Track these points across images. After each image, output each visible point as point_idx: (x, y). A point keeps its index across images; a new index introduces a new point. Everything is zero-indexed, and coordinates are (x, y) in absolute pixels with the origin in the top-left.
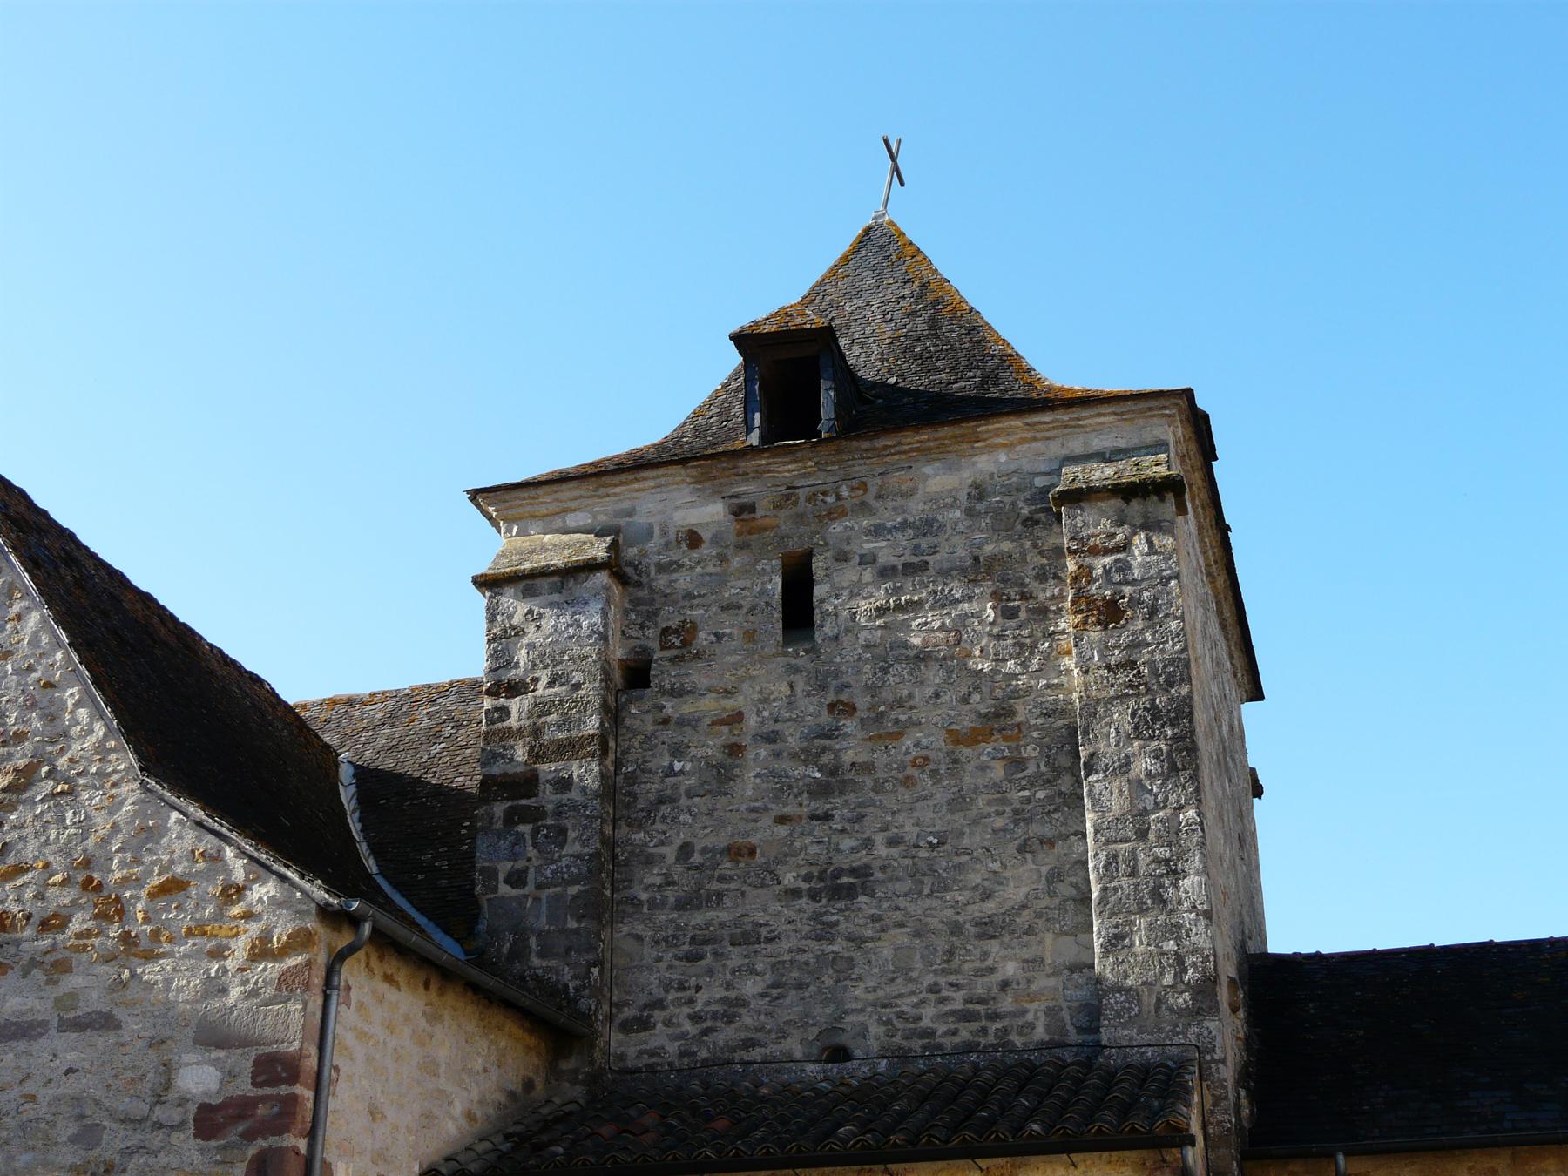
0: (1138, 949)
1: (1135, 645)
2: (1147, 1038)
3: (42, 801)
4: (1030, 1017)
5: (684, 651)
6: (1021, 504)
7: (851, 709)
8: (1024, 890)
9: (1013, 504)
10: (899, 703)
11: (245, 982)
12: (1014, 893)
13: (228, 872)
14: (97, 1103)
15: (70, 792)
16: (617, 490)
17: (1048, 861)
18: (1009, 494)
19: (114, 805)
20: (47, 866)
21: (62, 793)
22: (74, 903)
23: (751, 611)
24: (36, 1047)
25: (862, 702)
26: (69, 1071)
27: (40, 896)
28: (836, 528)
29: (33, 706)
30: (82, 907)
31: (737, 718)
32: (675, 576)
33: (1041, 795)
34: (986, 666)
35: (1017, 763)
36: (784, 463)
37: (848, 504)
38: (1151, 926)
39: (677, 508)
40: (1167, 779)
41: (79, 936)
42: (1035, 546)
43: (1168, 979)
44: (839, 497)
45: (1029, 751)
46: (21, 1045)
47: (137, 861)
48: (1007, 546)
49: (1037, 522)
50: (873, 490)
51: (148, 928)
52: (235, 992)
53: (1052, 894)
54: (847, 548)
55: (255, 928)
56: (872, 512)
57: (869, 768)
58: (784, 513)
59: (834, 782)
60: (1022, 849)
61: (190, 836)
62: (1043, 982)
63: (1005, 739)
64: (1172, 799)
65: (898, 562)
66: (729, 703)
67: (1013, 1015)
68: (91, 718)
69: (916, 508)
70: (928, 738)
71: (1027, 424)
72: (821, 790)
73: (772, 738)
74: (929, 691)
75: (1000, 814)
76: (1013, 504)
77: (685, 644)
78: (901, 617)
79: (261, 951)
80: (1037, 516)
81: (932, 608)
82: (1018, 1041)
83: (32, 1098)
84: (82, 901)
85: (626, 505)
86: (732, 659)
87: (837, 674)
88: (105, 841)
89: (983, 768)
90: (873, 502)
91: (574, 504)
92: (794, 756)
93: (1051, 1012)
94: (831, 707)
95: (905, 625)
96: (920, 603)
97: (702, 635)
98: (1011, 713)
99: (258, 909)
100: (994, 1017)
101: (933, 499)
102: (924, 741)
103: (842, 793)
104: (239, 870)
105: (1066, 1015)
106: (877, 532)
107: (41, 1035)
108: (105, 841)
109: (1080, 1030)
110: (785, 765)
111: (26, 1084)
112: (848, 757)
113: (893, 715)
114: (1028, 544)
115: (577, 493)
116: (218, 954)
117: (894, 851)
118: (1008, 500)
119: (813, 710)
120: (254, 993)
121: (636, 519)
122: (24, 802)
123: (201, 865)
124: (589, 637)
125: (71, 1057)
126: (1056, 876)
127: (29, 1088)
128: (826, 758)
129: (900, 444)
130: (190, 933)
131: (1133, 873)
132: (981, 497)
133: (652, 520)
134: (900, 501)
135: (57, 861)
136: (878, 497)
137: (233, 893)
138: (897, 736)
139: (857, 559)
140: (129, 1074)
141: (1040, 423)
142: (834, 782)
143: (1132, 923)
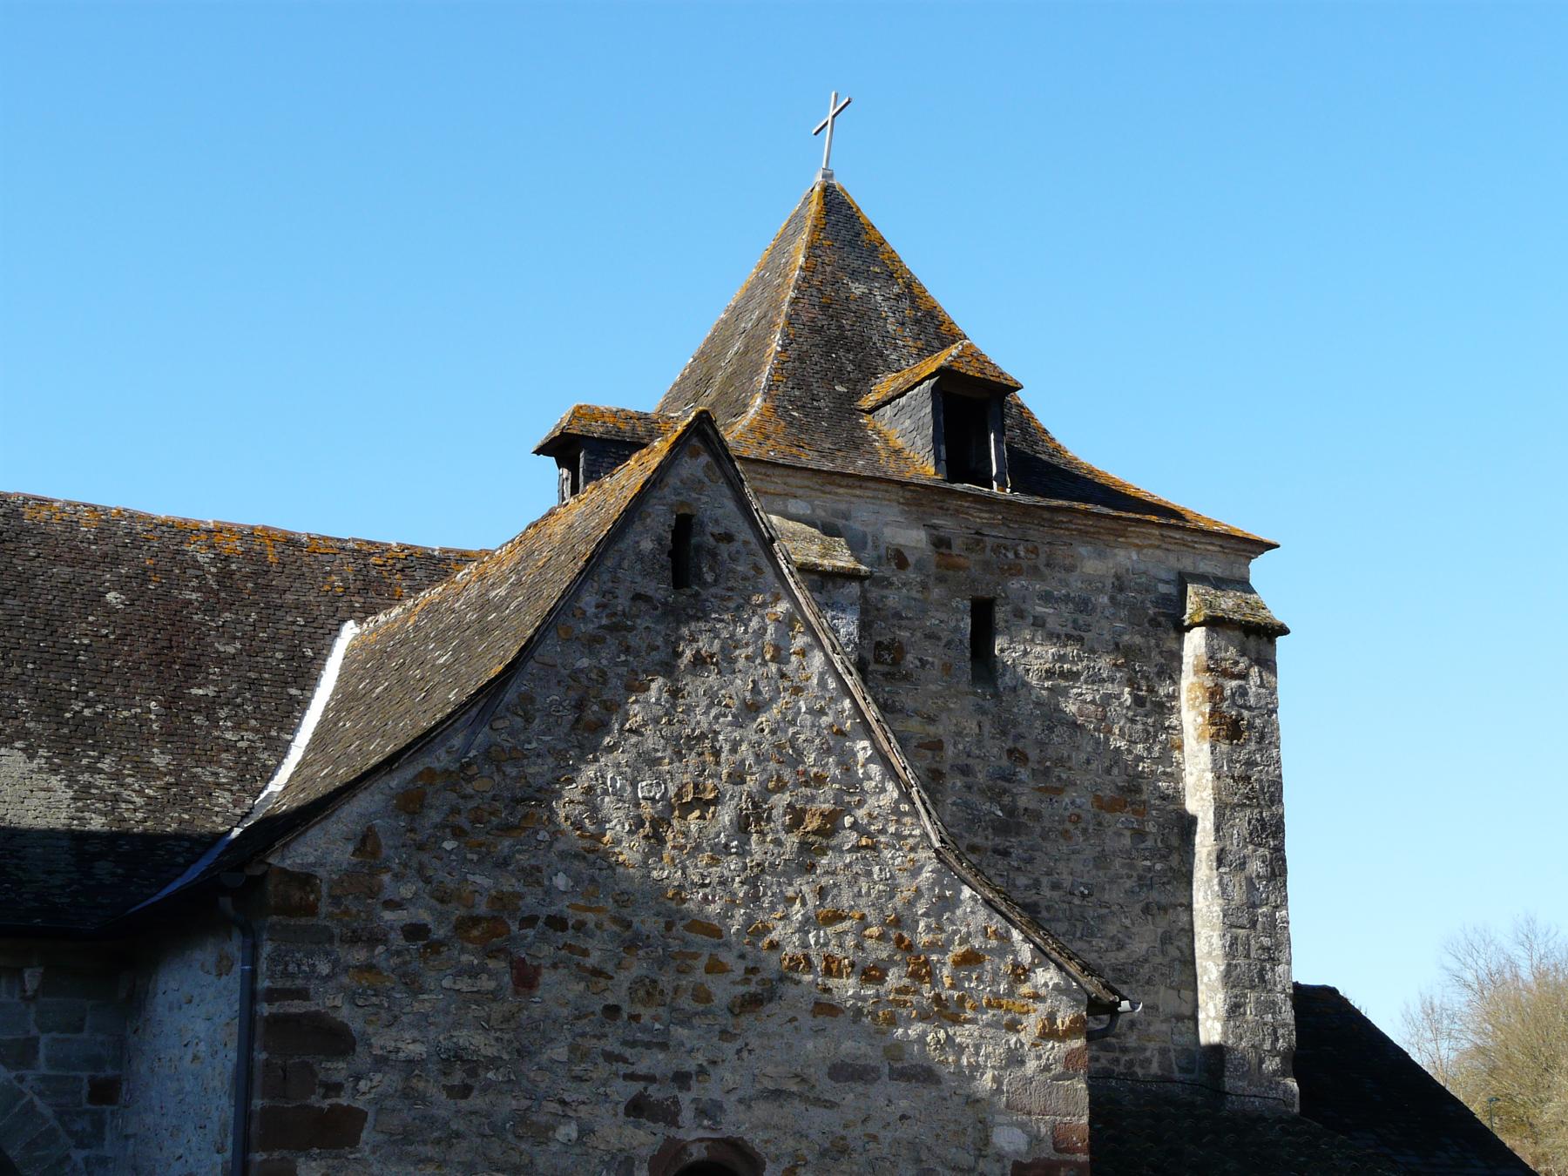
0: (1249, 1017)
1: (1250, 764)
2: (1254, 1090)
3: (849, 851)
4: (1148, 1054)
5: (893, 669)
7: (1022, 758)
8: (1145, 946)
9: (1142, 602)
10: (1060, 762)
11: (1039, 1057)
12: (1138, 947)
13: (1015, 953)
14: (929, 1149)
15: (873, 847)
16: (841, 491)
17: (1163, 923)
18: (1139, 592)
19: (915, 871)
20: (863, 917)
21: (866, 847)
22: (891, 962)
23: (948, 644)
24: (872, 1090)
25: (1033, 754)
26: (903, 1117)
27: (859, 946)
28: (1015, 584)
29: (829, 751)
30: (896, 964)
31: (936, 746)
32: (886, 592)
33: (1158, 867)
34: (1122, 744)
35: (1139, 835)
36: (981, 511)
37: (1024, 564)
39: (887, 524)
40: (1269, 882)
41: (899, 991)
42: (1158, 646)
43: (1267, 1046)
44: (1017, 555)
45: (1151, 827)
46: (859, 1087)
47: (941, 929)
48: (1138, 640)
49: (1159, 625)
50: (1043, 557)
51: (956, 994)
52: (1031, 1065)
53: (1164, 953)
54: (1023, 606)
55: (1043, 1008)
56: (1043, 579)
57: (1037, 816)
58: (974, 557)
59: (1011, 824)
60: (1146, 910)
61: (982, 913)
62: (1159, 1027)
63: (1135, 812)
64: (1272, 898)
65: (1063, 631)
66: (932, 729)
67: (1135, 1049)
68: (883, 775)
69: (1076, 586)
70: (1077, 798)
71: (1162, 535)
73: (965, 771)
74: (1083, 756)
75: (1130, 877)
76: (1142, 602)
77: (896, 662)
78: (1063, 683)
79: (1049, 1032)
80: (1162, 619)
81: (1086, 682)
82: (1140, 1072)
83: (874, 1138)
84: (897, 958)
85: (843, 506)
86: (932, 687)
87: (1015, 724)
88: (911, 904)
89: (1119, 834)
90: (1042, 568)
92: (982, 792)
93: (1163, 1052)
94: (1010, 752)
95: (1064, 692)
97: (909, 657)
98: (1138, 790)
99: (1043, 992)
100: (1124, 1050)
101: (1088, 580)
102: (1078, 801)
103: (1018, 834)
104: (1026, 953)
105: (1172, 1055)
106: (1047, 598)
107: (875, 1080)
108: (911, 904)
109: (1182, 1070)
110: (974, 798)
111: (870, 1123)
112: (1023, 802)
113: (1057, 771)
114: (1153, 642)
115: (806, 483)
116: (1013, 1026)
117: (1056, 895)
119: (995, 750)
120: (1047, 1068)
121: (851, 523)
122: (833, 848)
123: (993, 943)
124: (847, 645)
125: (904, 1103)
126: (1166, 939)
127: (872, 1128)
128: (1006, 799)
129: (1070, 522)
130: (989, 1005)
131: (1248, 956)
132: (1121, 589)
133: (868, 530)
134: (1063, 575)
135: (872, 916)
136: (1048, 565)
137: (1020, 973)
138: (1059, 791)
139: (1031, 620)
140: (952, 1126)
141: (1170, 537)
142: (1011, 824)
143: (1245, 996)
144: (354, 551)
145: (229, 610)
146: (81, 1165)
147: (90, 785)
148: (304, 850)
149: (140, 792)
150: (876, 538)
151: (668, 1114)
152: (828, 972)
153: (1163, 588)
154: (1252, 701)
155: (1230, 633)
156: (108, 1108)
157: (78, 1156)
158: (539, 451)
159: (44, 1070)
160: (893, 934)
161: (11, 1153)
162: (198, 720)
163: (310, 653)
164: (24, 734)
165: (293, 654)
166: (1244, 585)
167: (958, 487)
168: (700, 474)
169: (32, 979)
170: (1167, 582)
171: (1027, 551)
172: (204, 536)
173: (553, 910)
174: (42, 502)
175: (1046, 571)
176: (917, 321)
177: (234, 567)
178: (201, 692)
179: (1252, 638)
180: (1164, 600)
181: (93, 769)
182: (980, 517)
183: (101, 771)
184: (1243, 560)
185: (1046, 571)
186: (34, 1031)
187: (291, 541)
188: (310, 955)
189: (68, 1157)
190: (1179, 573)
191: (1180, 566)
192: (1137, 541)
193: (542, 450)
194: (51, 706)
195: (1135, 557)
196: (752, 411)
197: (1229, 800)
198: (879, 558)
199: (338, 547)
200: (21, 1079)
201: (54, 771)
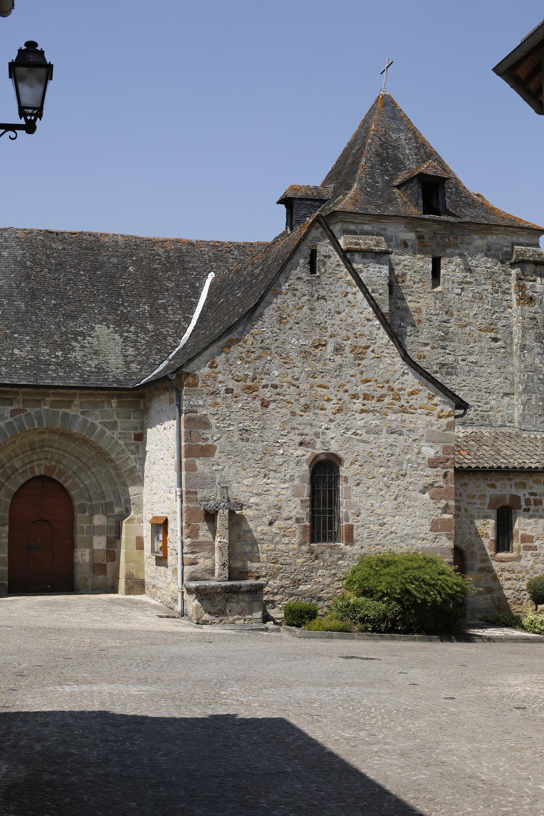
6: (500, 255)
18: (496, 251)
36: (435, 225)
38: (536, 398)
39: (400, 232)
44: (449, 240)
57: (456, 334)
72: (443, 339)
76: (498, 255)
91: (367, 222)
96: (471, 283)
118: (496, 253)
121: (387, 232)
133: (393, 234)
136: (461, 243)
143: (532, 396)
144: (212, 245)
145: (170, 271)
146: (133, 460)
147: (127, 337)
148: (193, 366)
149: (143, 339)
150: (396, 237)
151: (313, 446)
152: (364, 399)
154: (538, 290)
155: (530, 265)
156: (140, 442)
157: (132, 457)
158: (278, 203)
160: (386, 385)
161: (112, 456)
162: (162, 311)
163: (198, 285)
164: (105, 320)
165: (192, 286)
166: (537, 245)
167: (427, 216)
168: (319, 235)
170: (507, 247)
171: (453, 238)
172: (160, 244)
173: (273, 382)
174: (106, 235)
175: (460, 245)
176: (417, 148)
177: (171, 254)
178: (162, 301)
179: (538, 266)
180: (507, 252)
181: (128, 331)
182: (435, 227)
183: (130, 332)
185: (460, 245)
186: (116, 419)
187: (191, 244)
189: (129, 457)
190: (512, 243)
191: (512, 240)
194: (114, 308)
196: (353, 189)
197: (528, 327)
198: (398, 244)
199: (207, 244)
200: (113, 434)
201: (116, 333)
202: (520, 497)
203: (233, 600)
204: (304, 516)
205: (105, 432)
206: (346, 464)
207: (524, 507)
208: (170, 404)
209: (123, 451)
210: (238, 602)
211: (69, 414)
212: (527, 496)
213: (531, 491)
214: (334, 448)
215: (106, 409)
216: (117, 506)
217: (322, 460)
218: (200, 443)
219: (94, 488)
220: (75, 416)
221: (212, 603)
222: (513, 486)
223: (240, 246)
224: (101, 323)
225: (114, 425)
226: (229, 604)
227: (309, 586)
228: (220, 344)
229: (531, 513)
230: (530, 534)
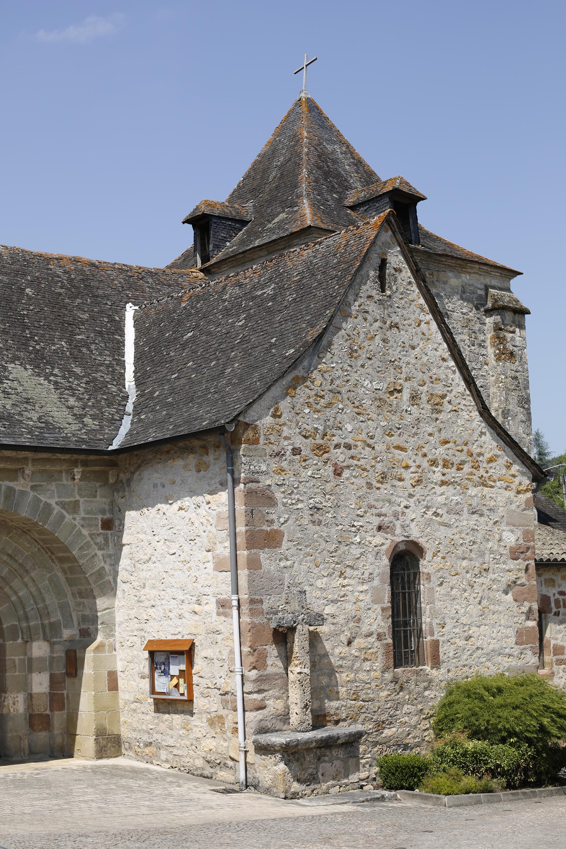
6: (474, 299)
71: (479, 268)
76: (472, 298)
118: (471, 296)
129: (446, 261)
134: (443, 286)
136: (437, 281)
141: (483, 269)
144: (119, 269)
145: (78, 298)
146: (101, 558)
148: (252, 414)
152: (444, 466)
153: (480, 292)
154: (517, 344)
156: (109, 532)
157: (100, 553)
159: (83, 515)
161: (74, 553)
162: (84, 350)
163: (117, 318)
166: (509, 290)
168: (389, 240)
169: (78, 472)
170: (481, 290)
171: (430, 274)
173: (346, 441)
175: (437, 283)
177: (73, 276)
178: (80, 337)
180: (480, 296)
184: (508, 280)
185: (437, 283)
186: (78, 498)
187: (92, 265)
188: (258, 462)
189: (96, 554)
190: (485, 285)
191: (485, 282)
192: (469, 270)
193: (187, 221)
194: (24, 344)
195: (468, 278)
197: (510, 388)
200: (74, 519)
202: (549, 597)
203: (326, 758)
204: (386, 631)
205: (63, 517)
206: (428, 556)
207: (554, 610)
208: (199, 471)
209: (88, 545)
210: (331, 761)
211: (15, 490)
212: (557, 596)
213: (560, 589)
214: (415, 534)
215: (65, 482)
216: (66, 627)
217: (401, 551)
218: (265, 528)
219: (32, 602)
220: (23, 493)
221: (302, 765)
222: (543, 583)
223: (152, 272)
224: (13, 362)
225: (74, 507)
226: (321, 765)
227: (394, 730)
228: (284, 383)
229: (561, 617)
230: (561, 644)
